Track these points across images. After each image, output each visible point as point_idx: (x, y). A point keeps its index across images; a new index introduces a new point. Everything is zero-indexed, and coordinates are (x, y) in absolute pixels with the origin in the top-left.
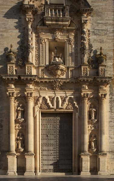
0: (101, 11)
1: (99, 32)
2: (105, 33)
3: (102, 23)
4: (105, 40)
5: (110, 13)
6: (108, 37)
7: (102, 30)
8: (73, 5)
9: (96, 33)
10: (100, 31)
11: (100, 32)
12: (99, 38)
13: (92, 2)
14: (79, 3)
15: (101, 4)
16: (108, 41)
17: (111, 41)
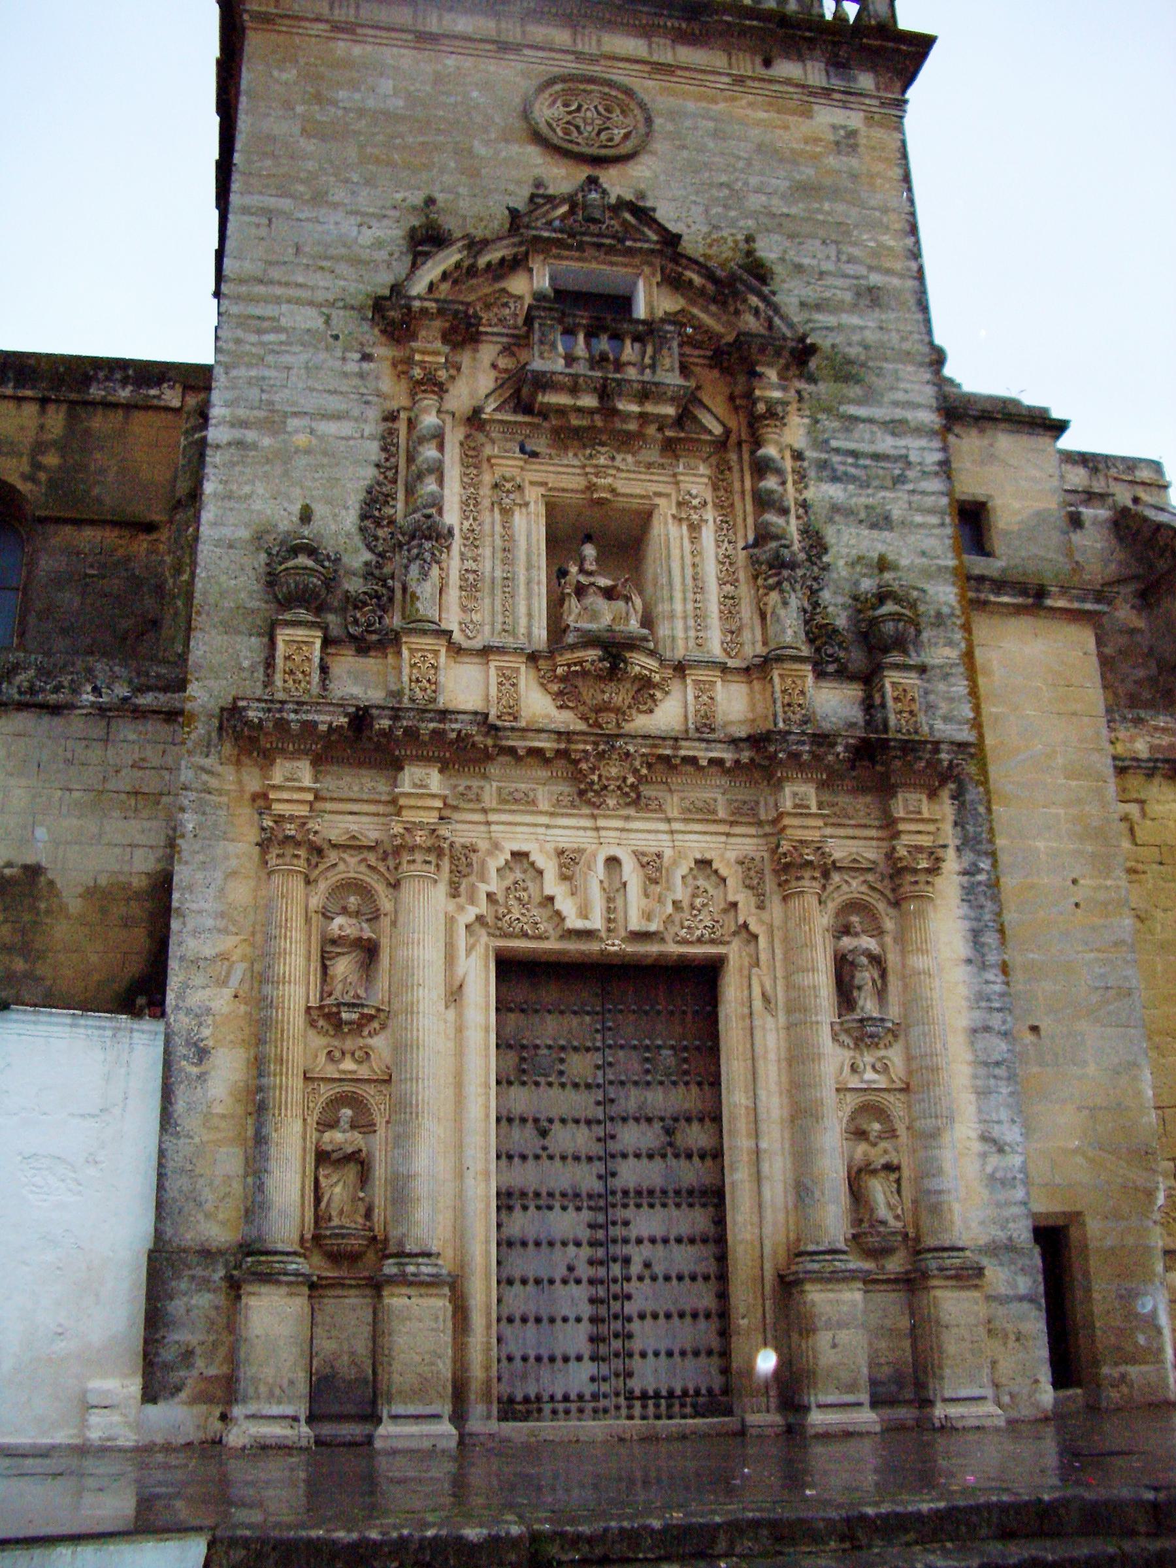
0: (858, 354)
1: (856, 466)
2: (897, 472)
3: (870, 421)
4: (896, 513)
5: (910, 368)
6: (916, 498)
7: (876, 457)
8: (695, 311)
9: (841, 468)
10: (862, 462)
11: (865, 467)
12: (863, 500)
13: (803, 305)
14: (732, 309)
15: (855, 320)
16: (919, 519)
17: (934, 520)
